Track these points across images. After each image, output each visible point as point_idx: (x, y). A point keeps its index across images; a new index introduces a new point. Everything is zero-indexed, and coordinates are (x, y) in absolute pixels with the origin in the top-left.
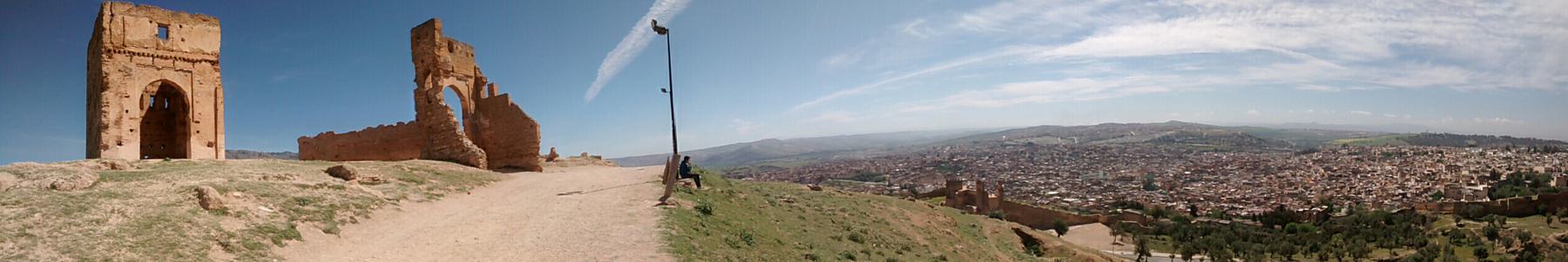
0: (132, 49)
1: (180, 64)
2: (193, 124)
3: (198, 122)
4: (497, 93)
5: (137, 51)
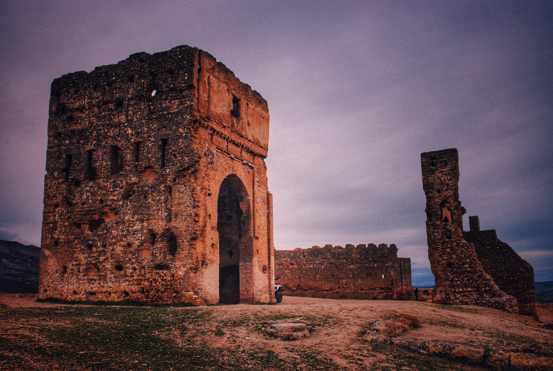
0: (215, 126)
1: (244, 153)
2: (255, 241)
3: (257, 238)
4: (483, 227)
5: (218, 128)
